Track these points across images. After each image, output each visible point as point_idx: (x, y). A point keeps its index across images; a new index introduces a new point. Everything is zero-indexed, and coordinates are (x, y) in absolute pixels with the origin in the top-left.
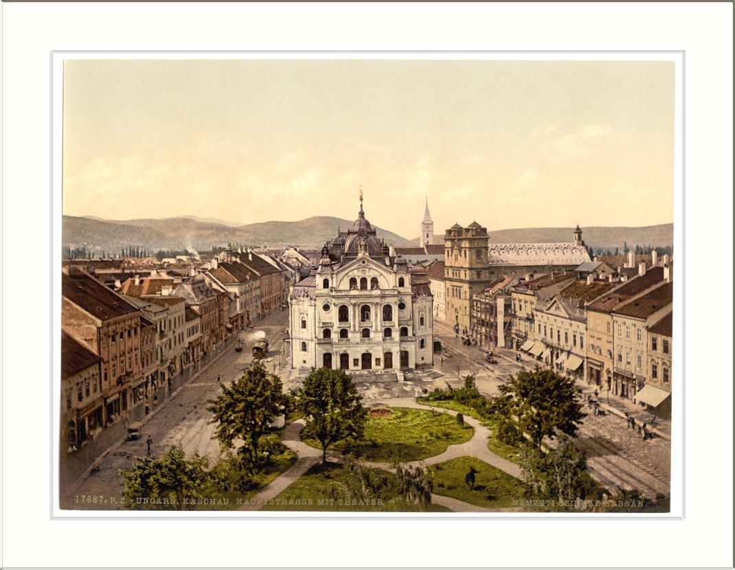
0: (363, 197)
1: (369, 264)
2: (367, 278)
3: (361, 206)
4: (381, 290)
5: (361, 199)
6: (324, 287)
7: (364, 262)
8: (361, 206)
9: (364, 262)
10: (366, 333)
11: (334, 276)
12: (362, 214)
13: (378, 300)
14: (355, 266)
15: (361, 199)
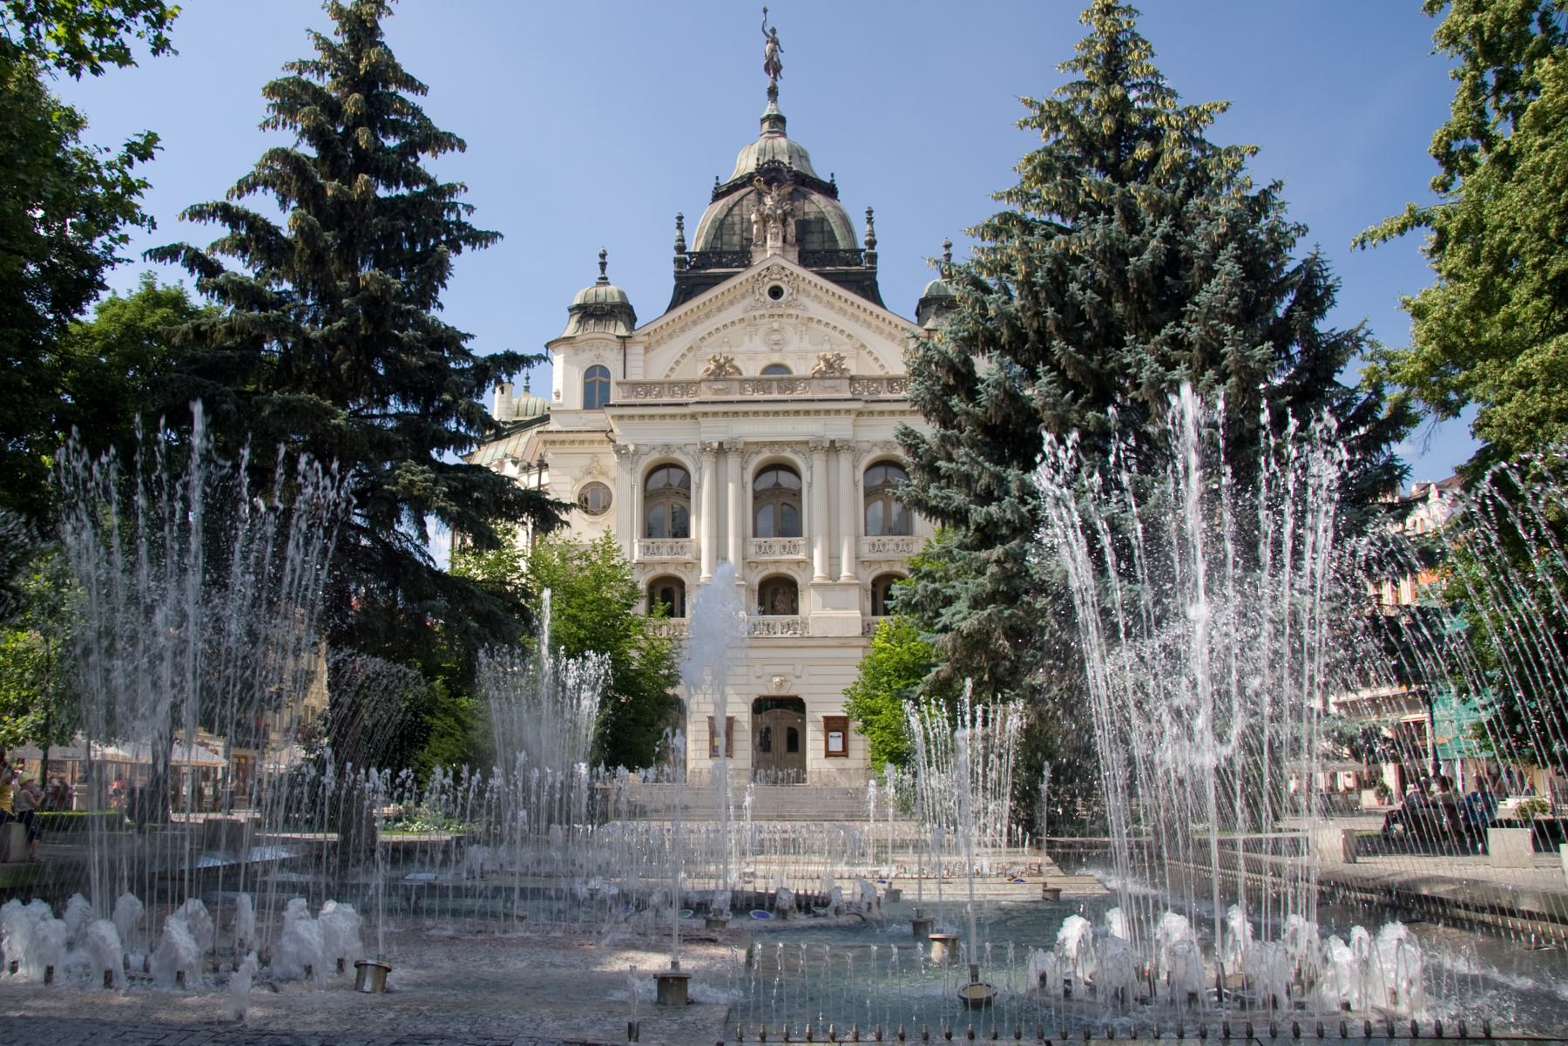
0: (783, 58)
1: (803, 299)
2: (789, 363)
3: (773, 93)
4: (852, 379)
5: (773, 67)
6: (588, 404)
7: (776, 293)
8: (773, 93)
9: (776, 293)
10: (778, 594)
11: (636, 351)
12: (777, 122)
13: (839, 428)
14: (735, 312)
15: (773, 67)
